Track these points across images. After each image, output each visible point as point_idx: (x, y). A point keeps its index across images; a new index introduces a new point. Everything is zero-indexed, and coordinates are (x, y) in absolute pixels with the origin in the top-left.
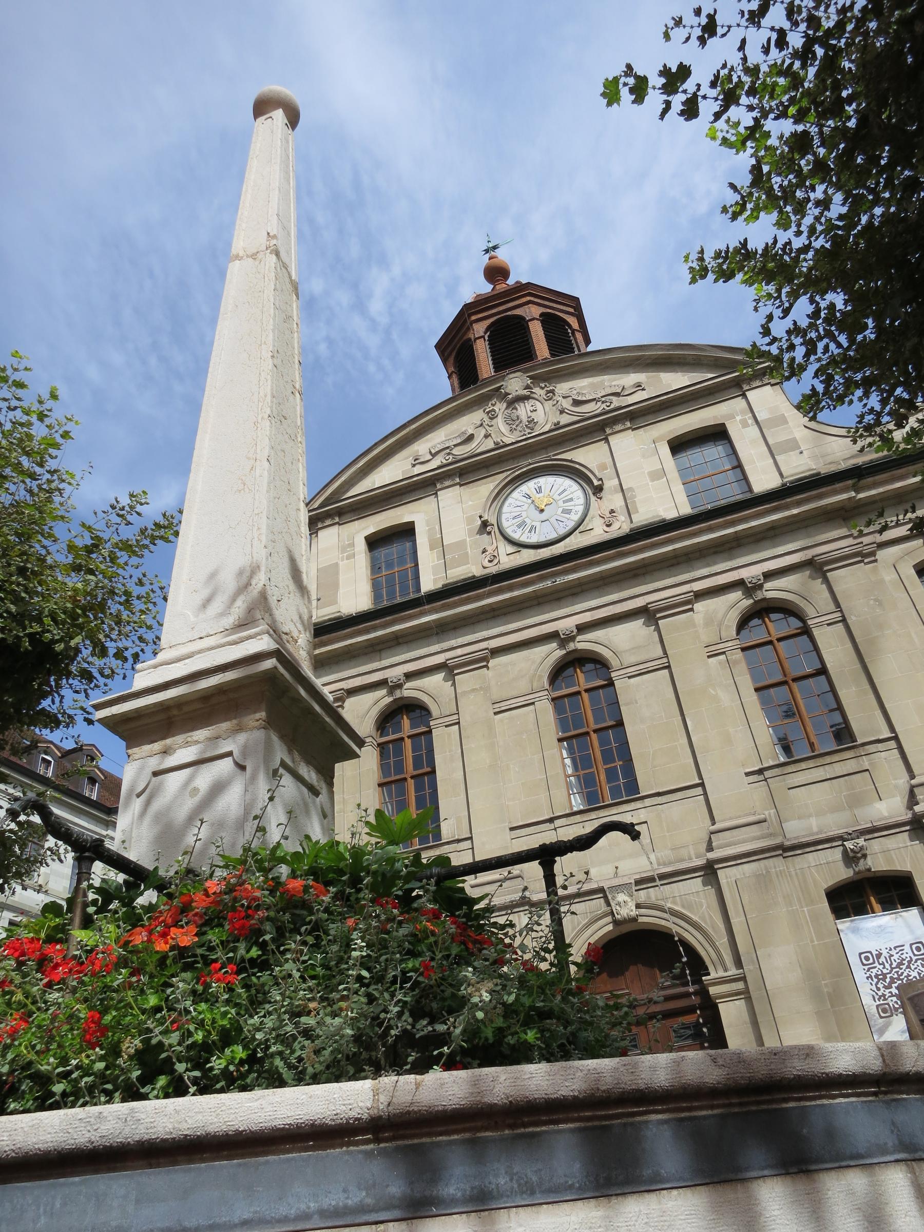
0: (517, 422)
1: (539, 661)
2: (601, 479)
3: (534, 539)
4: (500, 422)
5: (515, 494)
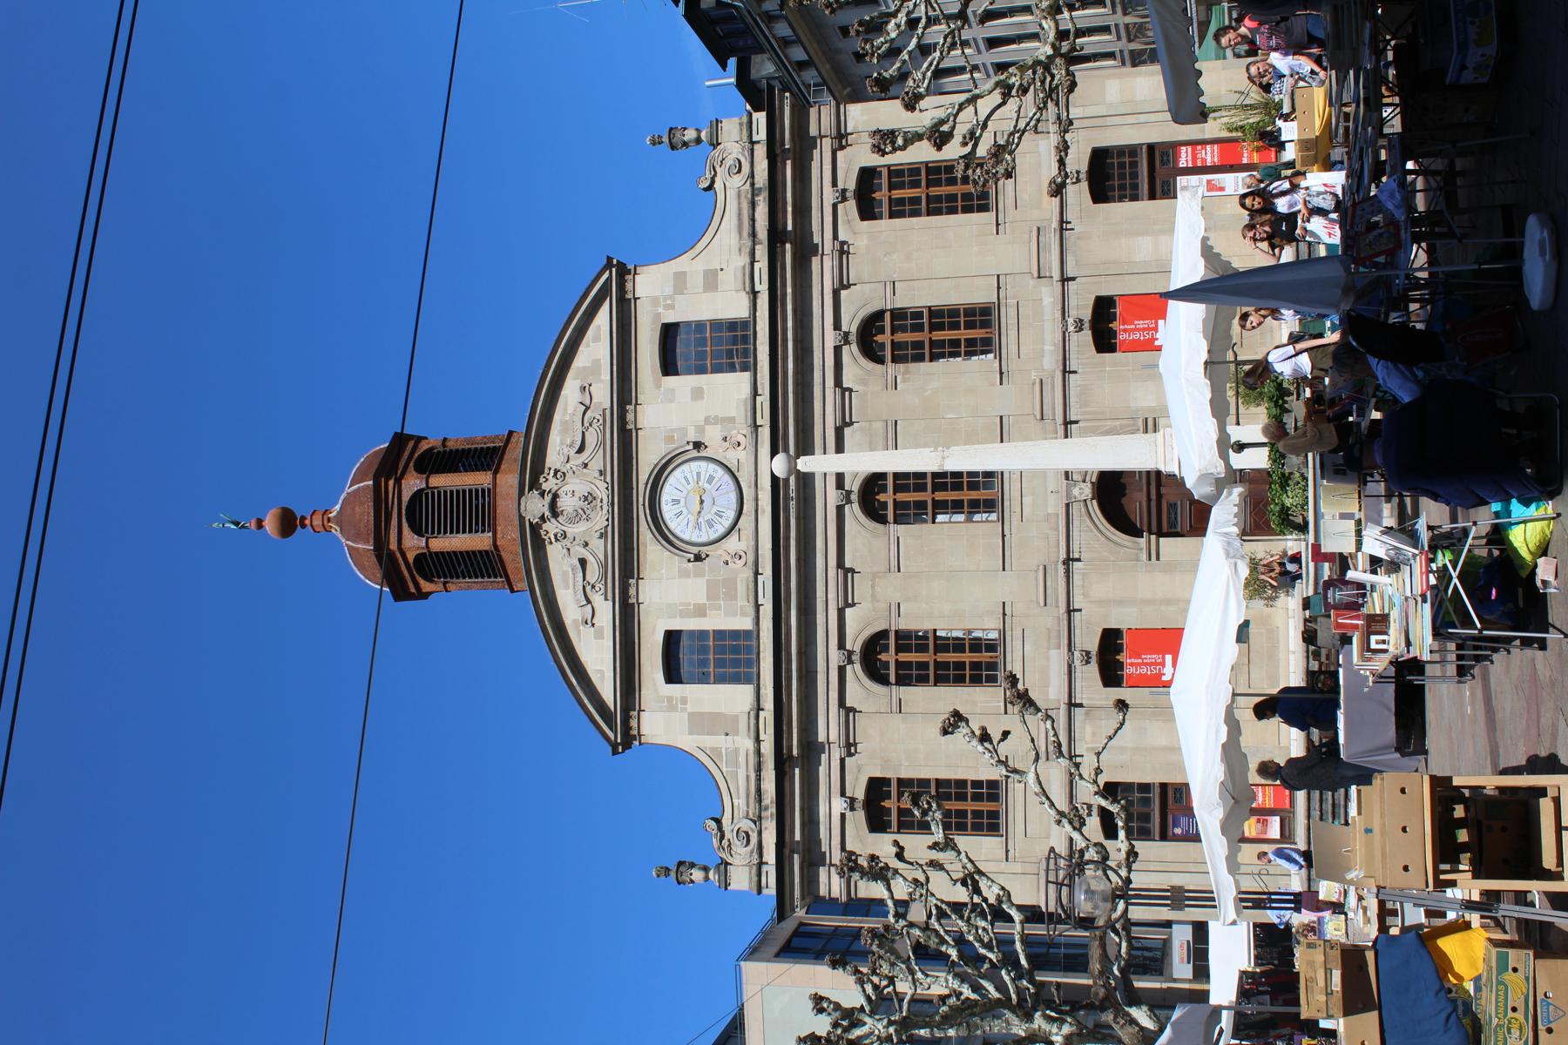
0: (580, 511)
1: (859, 528)
2: (688, 443)
3: (731, 515)
4: (572, 530)
5: (672, 526)
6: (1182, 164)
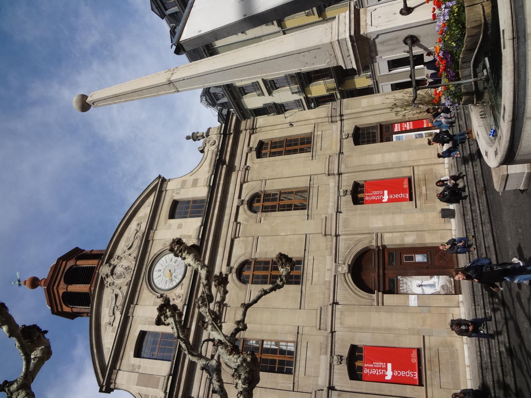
0: (122, 273)
3: (180, 277)
5: (155, 281)
6: (396, 130)
